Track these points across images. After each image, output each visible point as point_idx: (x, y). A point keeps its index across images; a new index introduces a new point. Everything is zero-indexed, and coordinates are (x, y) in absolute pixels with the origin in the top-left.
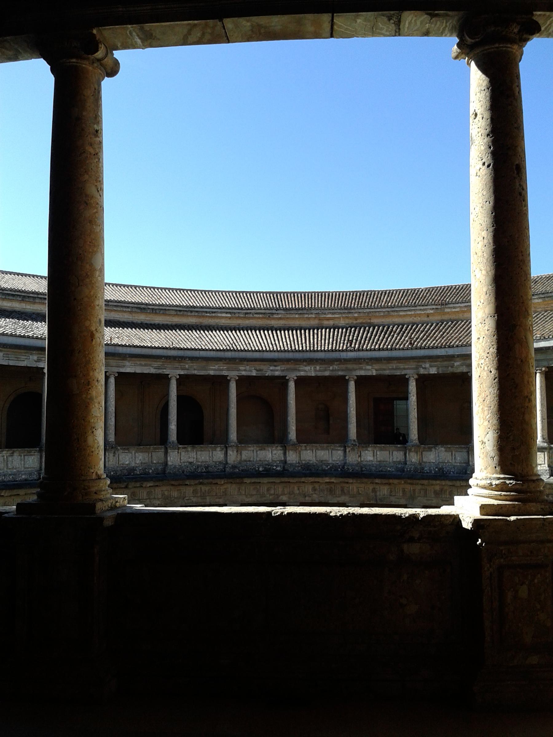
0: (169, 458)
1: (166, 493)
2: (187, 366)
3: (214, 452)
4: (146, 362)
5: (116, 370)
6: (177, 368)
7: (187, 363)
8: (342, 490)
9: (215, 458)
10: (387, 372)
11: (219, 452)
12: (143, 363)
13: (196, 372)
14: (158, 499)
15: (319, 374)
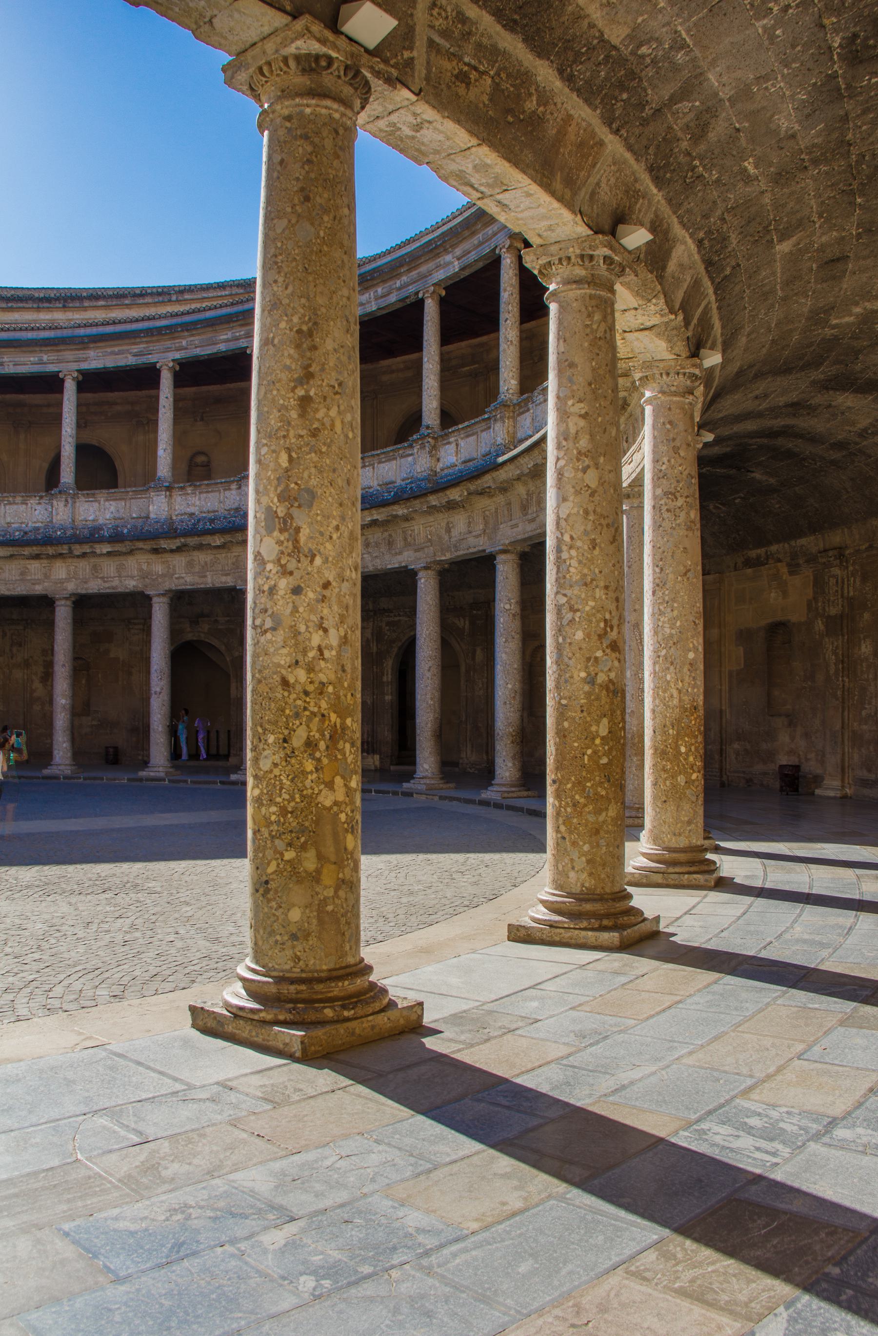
0: (151, 508)
1: (145, 567)
2: (184, 343)
3: (227, 493)
4: (120, 348)
5: (75, 366)
6: (168, 350)
7: (184, 338)
8: (405, 539)
9: (228, 502)
10: (473, 256)
11: (234, 492)
12: (116, 349)
13: (198, 352)
14: (132, 577)
15: (383, 303)
